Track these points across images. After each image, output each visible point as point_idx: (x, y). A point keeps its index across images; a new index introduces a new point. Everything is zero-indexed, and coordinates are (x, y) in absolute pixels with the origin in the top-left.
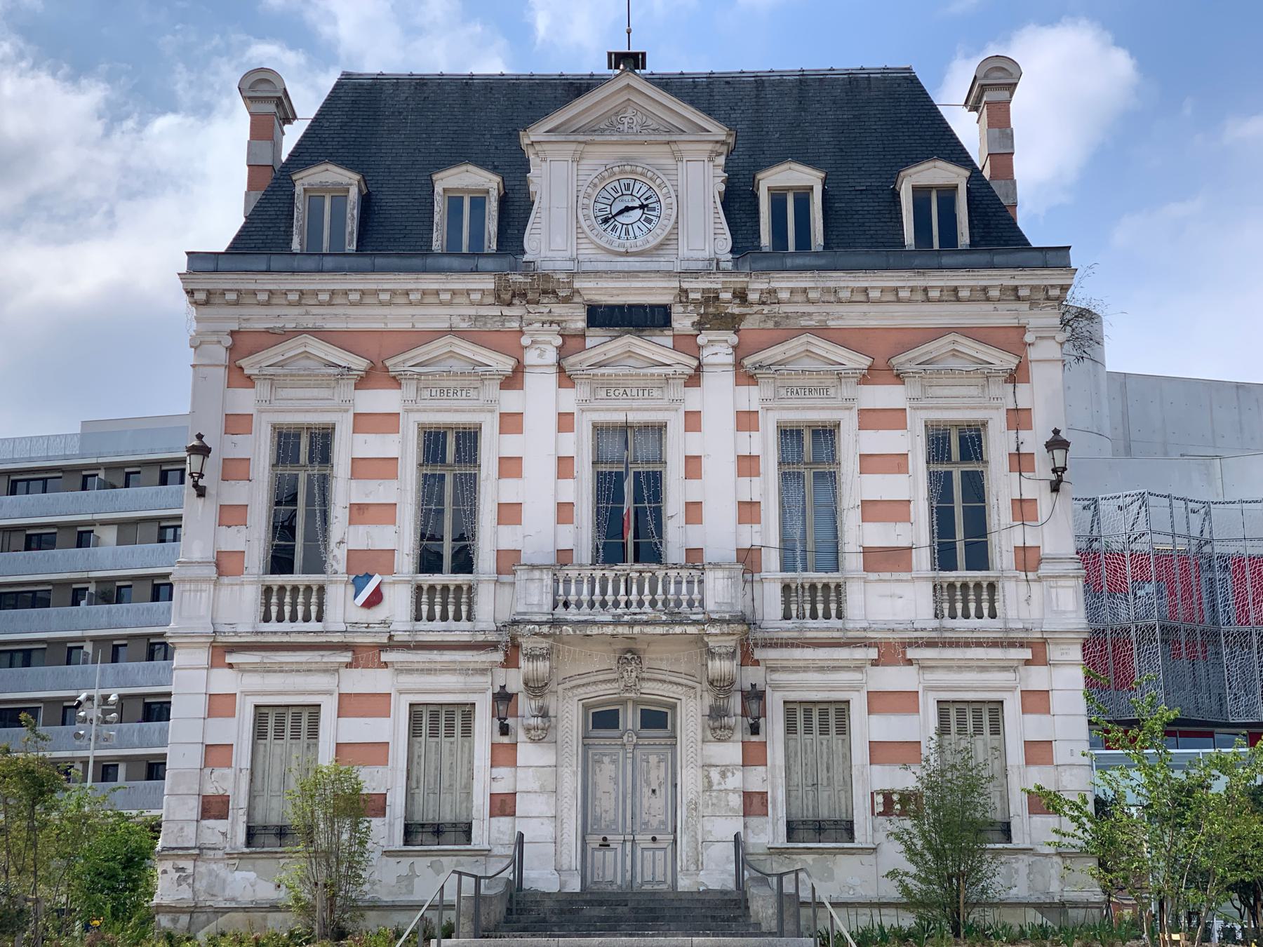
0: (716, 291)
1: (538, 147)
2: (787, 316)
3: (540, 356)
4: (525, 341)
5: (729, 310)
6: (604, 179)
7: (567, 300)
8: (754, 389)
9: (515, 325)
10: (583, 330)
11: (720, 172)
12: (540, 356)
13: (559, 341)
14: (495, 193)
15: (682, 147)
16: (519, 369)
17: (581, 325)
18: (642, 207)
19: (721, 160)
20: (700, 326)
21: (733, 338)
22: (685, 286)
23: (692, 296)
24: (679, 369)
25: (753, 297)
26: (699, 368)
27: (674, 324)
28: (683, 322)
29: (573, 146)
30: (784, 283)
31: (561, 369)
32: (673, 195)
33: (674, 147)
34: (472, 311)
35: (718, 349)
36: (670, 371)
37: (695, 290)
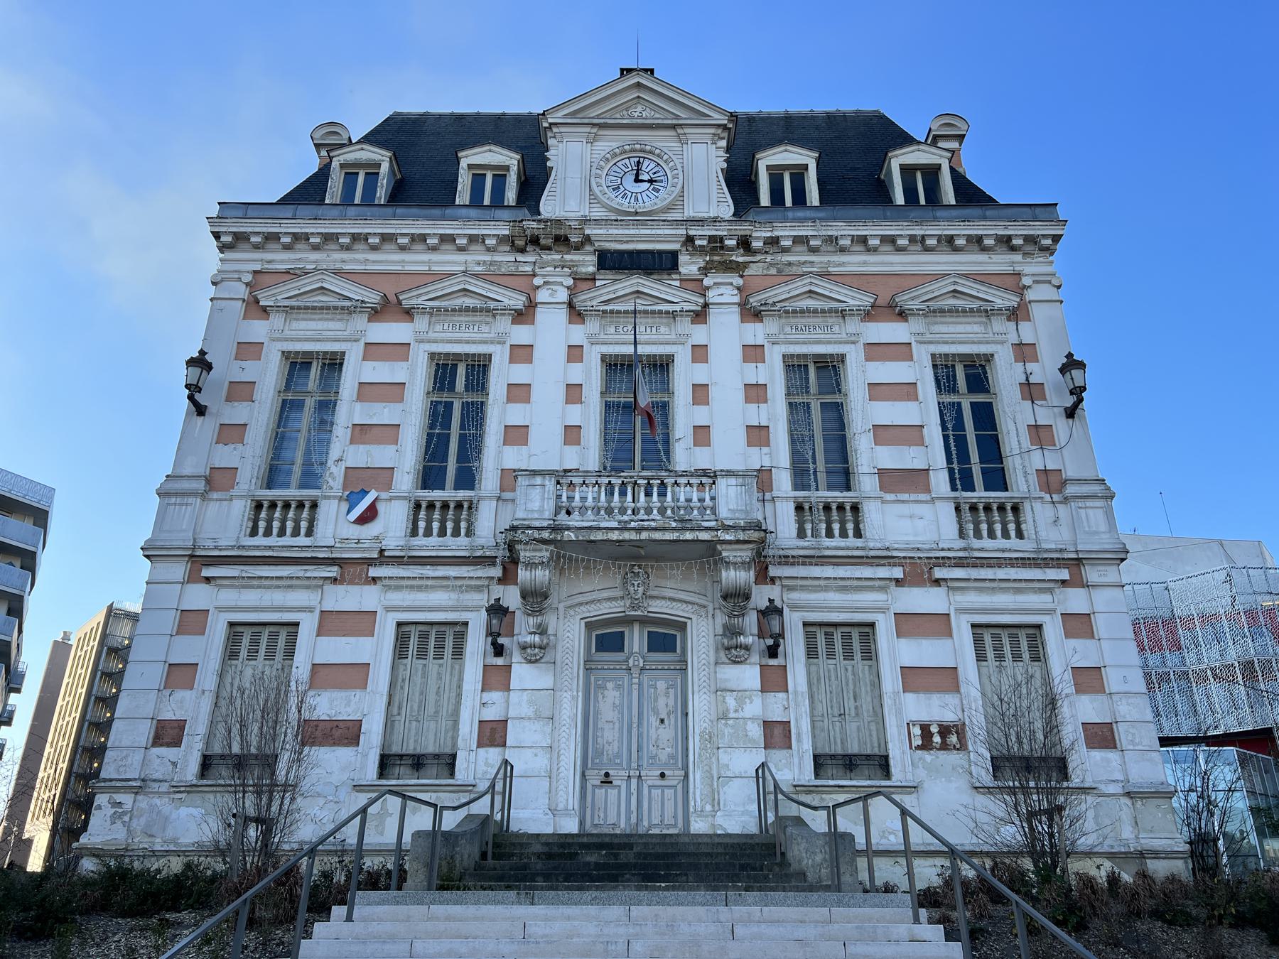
0: (721, 239)
1: (555, 130)
2: (790, 264)
3: (551, 295)
4: (537, 281)
5: (734, 258)
6: (615, 155)
7: (578, 247)
8: (759, 326)
9: (528, 268)
10: (594, 274)
11: (722, 153)
12: (551, 295)
13: (570, 282)
14: (516, 168)
15: (687, 130)
16: (532, 305)
17: (592, 269)
18: (651, 181)
19: (723, 143)
20: (705, 270)
21: (738, 281)
22: (691, 233)
23: (698, 243)
24: (687, 307)
25: (757, 244)
26: (706, 306)
27: (681, 269)
28: (689, 266)
29: (588, 130)
30: (785, 232)
31: (571, 305)
32: (679, 166)
33: (680, 131)
34: (488, 258)
35: (724, 291)
36: (677, 308)
37: (701, 238)
